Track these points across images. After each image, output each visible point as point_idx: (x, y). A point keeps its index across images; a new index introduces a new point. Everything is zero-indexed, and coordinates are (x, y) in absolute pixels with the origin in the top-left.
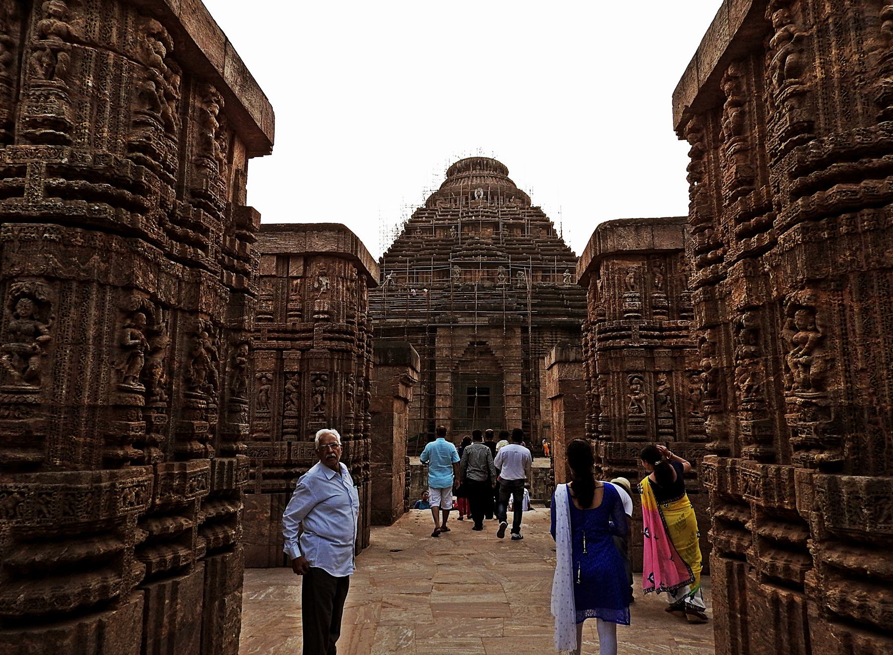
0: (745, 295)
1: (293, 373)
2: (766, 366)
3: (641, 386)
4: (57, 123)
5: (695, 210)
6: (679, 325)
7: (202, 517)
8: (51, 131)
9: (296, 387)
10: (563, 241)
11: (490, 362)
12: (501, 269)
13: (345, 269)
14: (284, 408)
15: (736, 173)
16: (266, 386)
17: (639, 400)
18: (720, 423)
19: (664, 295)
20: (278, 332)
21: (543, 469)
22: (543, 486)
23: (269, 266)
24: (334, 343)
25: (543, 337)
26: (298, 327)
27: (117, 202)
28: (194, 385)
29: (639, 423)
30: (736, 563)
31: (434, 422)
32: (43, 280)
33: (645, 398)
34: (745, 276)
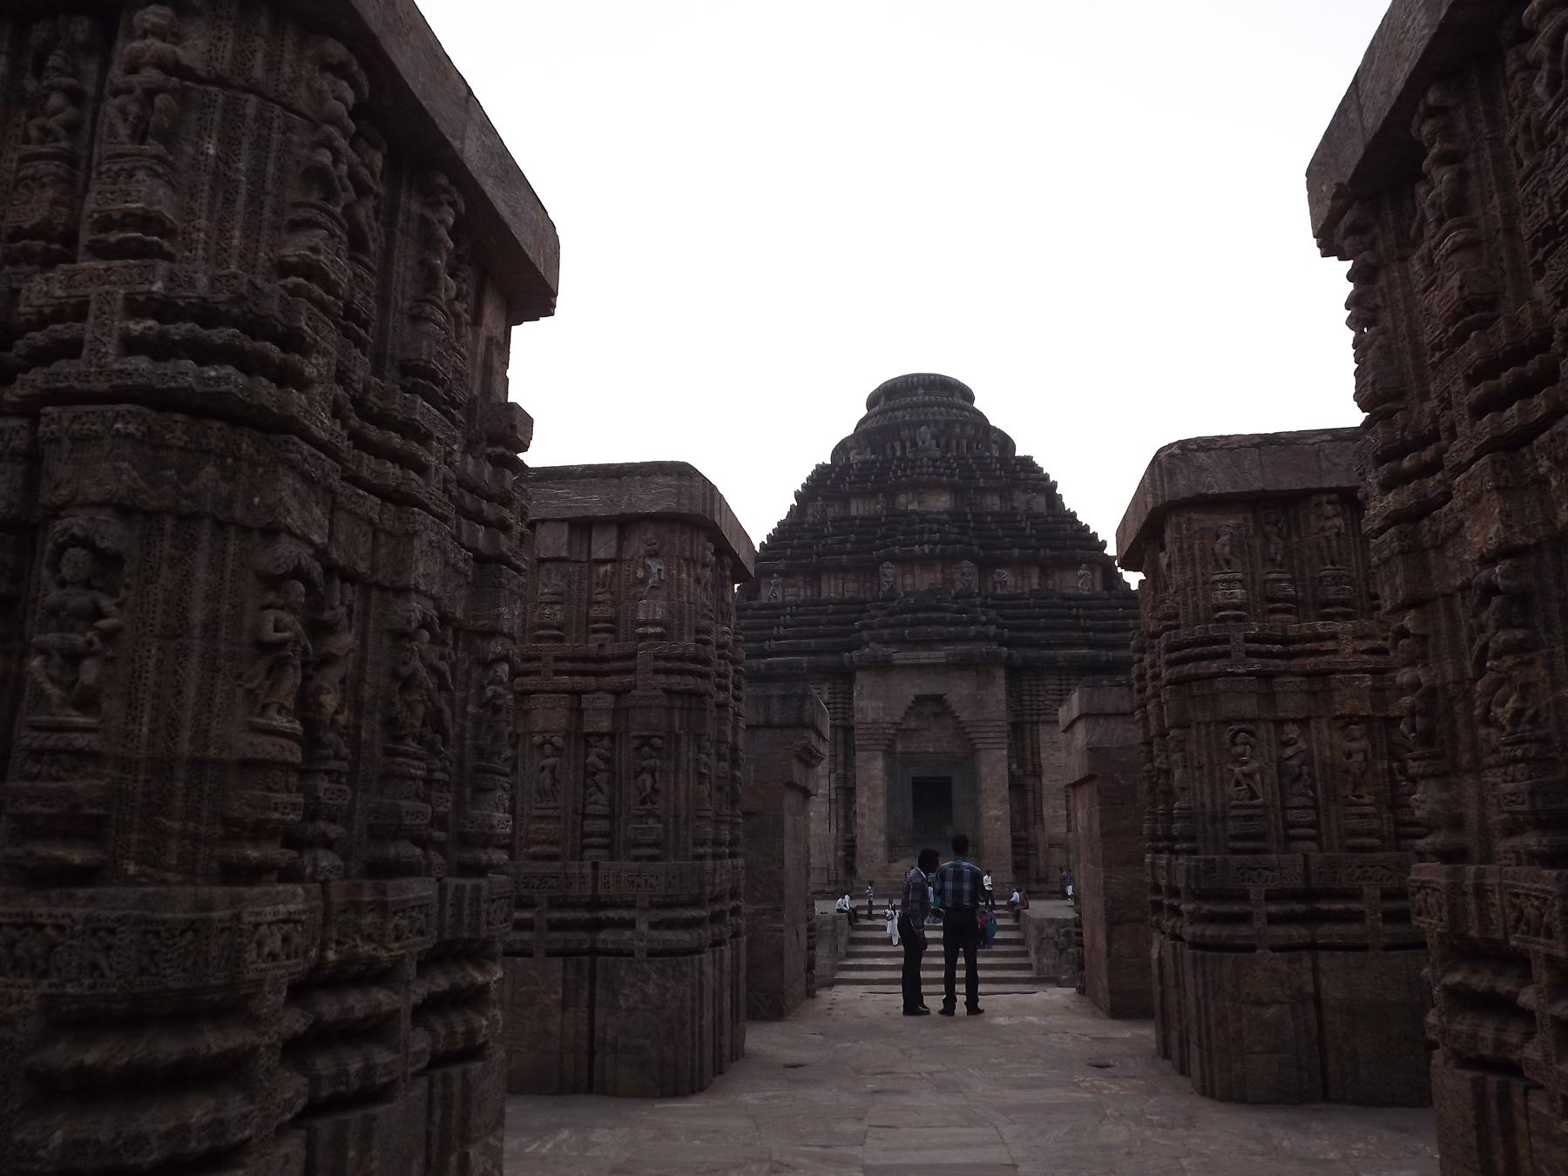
0: (1499, 525)
1: (600, 736)
2: (1551, 668)
3: (1253, 748)
4: (147, 221)
5: (1370, 378)
6: (1320, 630)
7: (420, 991)
8: (136, 234)
9: (607, 761)
10: (1074, 515)
12: (967, 566)
13: (692, 544)
14: (585, 798)
15: (1461, 288)
16: (551, 761)
17: (1249, 775)
18: (1445, 796)
19: (1288, 576)
20: (572, 659)
21: (1053, 919)
22: (1053, 950)
23: (553, 541)
24: (675, 680)
26: (609, 650)
27: (248, 364)
28: (403, 732)
29: (1249, 818)
30: (1493, 1081)
31: (854, 841)
32: (109, 511)
33: (1262, 770)
34: (1497, 488)
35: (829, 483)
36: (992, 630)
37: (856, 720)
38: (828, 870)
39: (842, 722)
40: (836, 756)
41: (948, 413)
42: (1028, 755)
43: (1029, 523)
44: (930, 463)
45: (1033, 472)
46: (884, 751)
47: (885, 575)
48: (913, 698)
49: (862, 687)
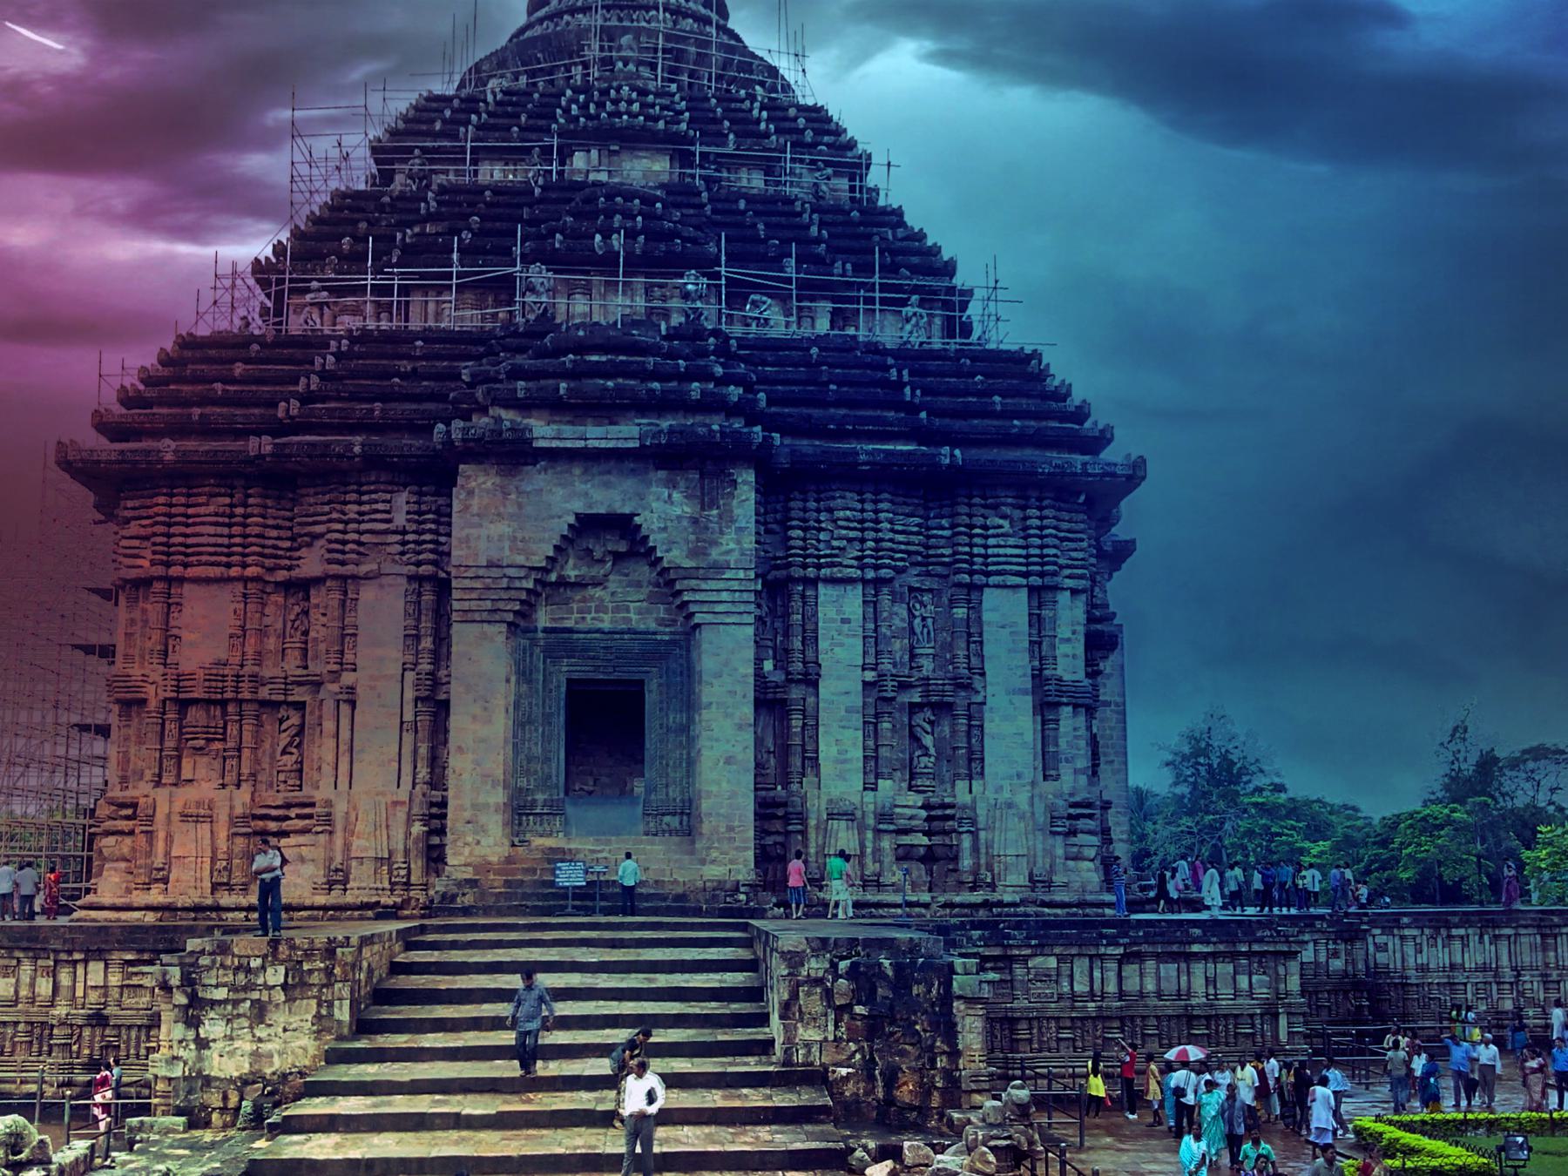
10: (899, 213)
11: (646, 591)
25: (830, 510)
31: (443, 804)
35: (438, 126)
36: (735, 392)
37: (454, 561)
38: (389, 860)
39: (430, 568)
40: (418, 638)
41: (675, 23)
42: (797, 644)
43: (815, 216)
44: (634, 95)
45: (829, 133)
46: (510, 624)
47: (531, 289)
48: (571, 520)
49: (471, 493)
